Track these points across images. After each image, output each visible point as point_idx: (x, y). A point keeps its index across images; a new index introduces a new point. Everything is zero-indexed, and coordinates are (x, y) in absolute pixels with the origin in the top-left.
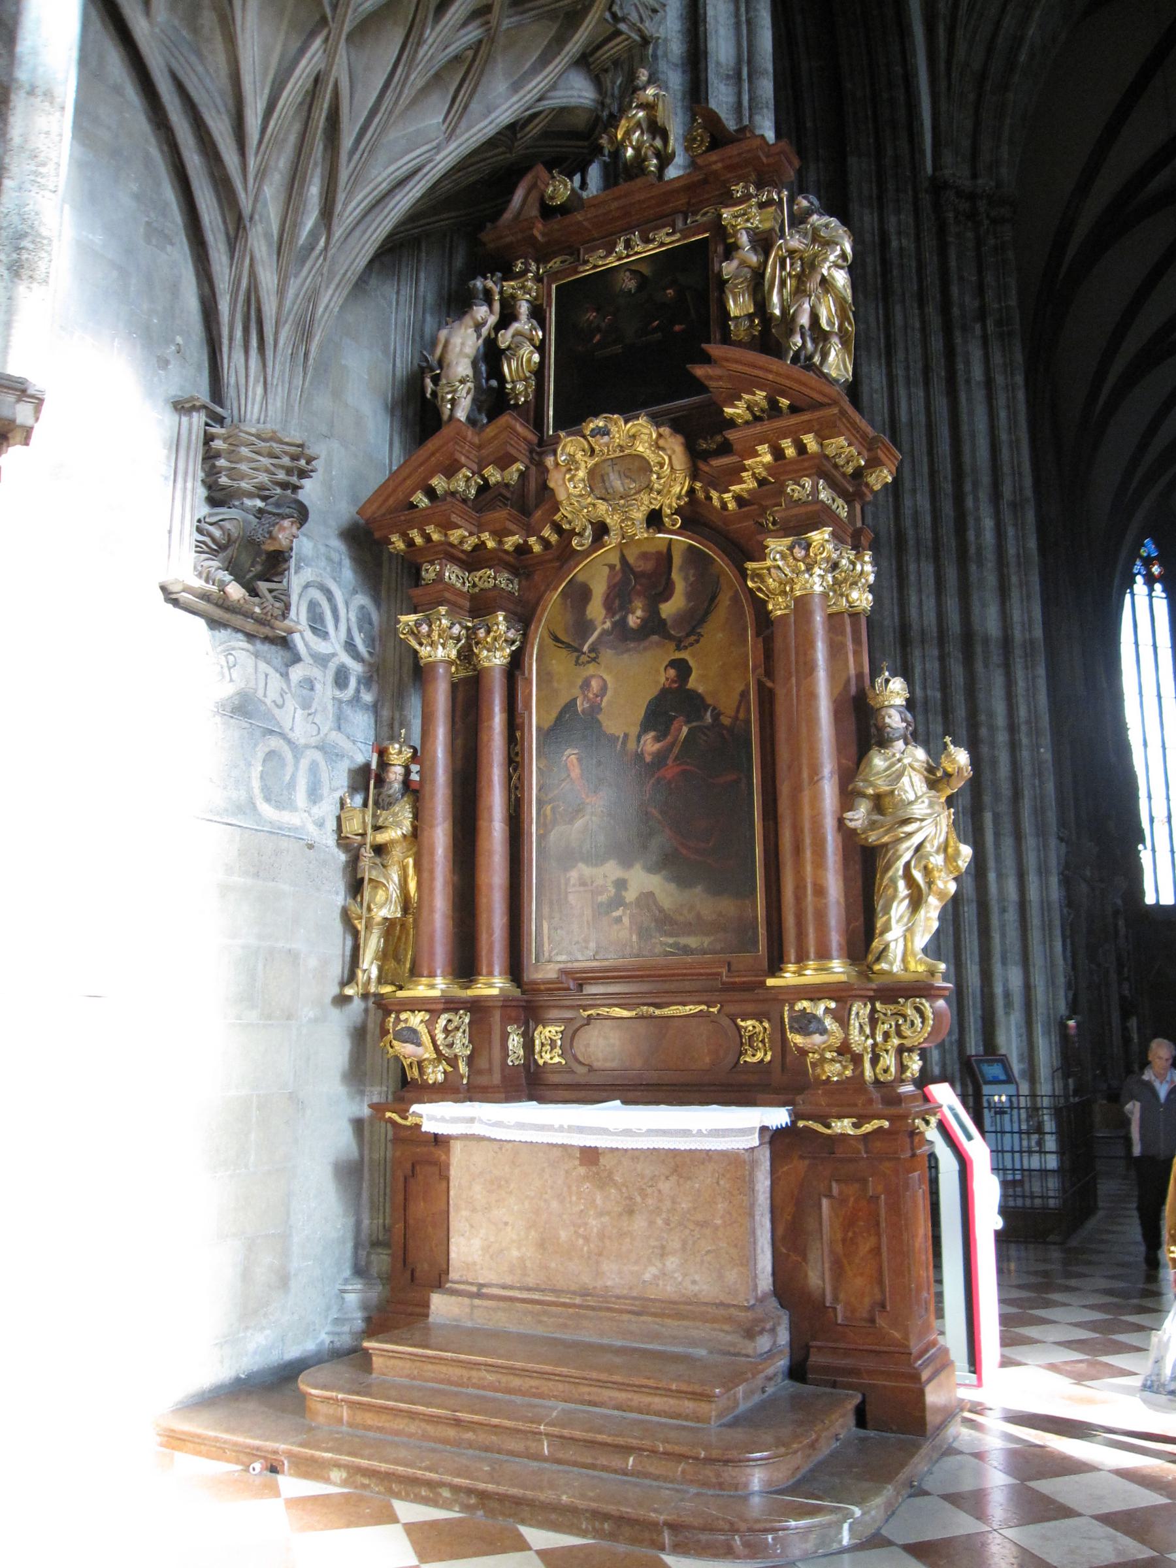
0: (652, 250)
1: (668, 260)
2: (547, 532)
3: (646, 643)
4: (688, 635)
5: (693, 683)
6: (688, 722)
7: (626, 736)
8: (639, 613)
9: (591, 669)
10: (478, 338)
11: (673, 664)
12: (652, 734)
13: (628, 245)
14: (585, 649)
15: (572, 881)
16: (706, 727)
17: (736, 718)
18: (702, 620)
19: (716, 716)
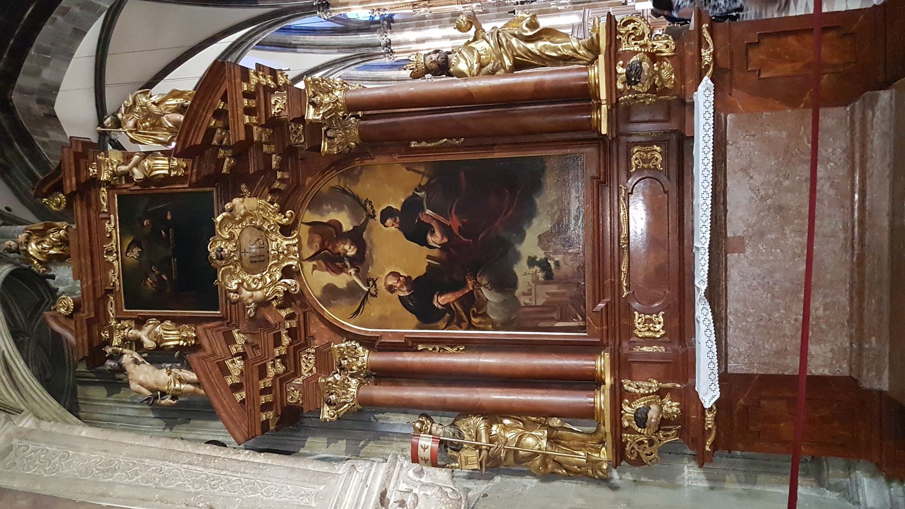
0: (116, 235)
1: (125, 224)
2: (284, 313)
3: (368, 242)
4: (365, 209)
5: (397, 206)
6: (423, 211)
7: (429, 257)
8: (347, 247)
9: (381, 285)
10: (145, 363)
11: (383, 221)
12: (429, 237)
13: (110, 253)
14: (366, 289)
15: (527, 301)
16: (427, 196)
17: (423, 174)
18: (356, 198)
19: (420, 188)
